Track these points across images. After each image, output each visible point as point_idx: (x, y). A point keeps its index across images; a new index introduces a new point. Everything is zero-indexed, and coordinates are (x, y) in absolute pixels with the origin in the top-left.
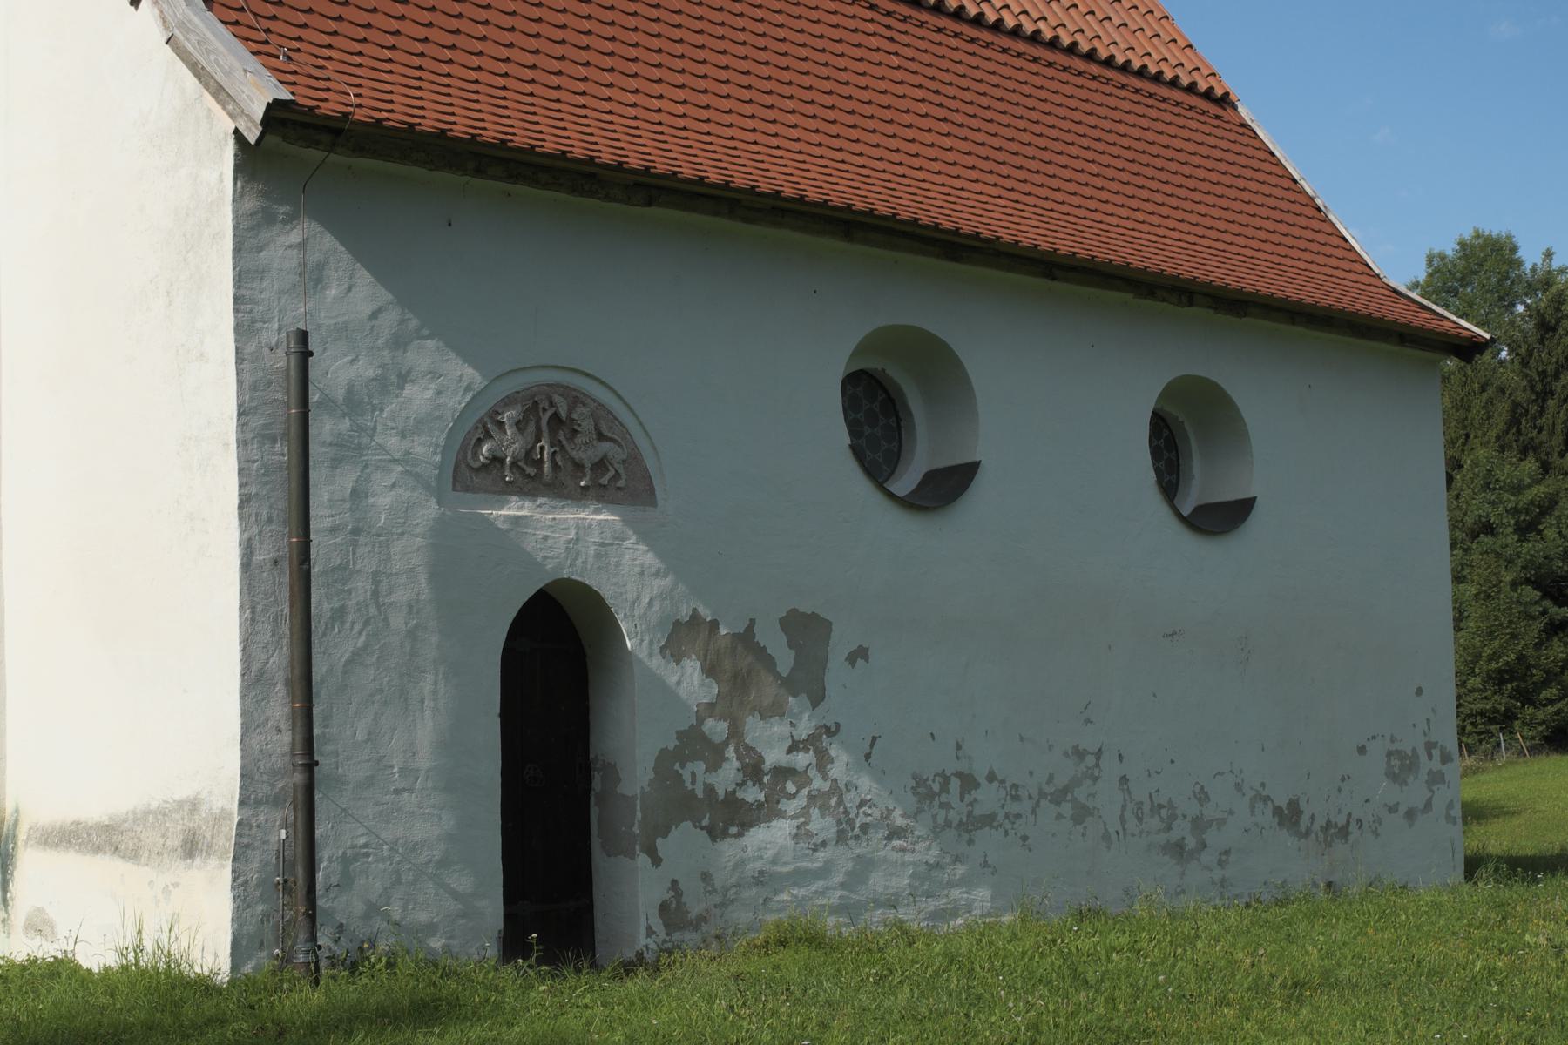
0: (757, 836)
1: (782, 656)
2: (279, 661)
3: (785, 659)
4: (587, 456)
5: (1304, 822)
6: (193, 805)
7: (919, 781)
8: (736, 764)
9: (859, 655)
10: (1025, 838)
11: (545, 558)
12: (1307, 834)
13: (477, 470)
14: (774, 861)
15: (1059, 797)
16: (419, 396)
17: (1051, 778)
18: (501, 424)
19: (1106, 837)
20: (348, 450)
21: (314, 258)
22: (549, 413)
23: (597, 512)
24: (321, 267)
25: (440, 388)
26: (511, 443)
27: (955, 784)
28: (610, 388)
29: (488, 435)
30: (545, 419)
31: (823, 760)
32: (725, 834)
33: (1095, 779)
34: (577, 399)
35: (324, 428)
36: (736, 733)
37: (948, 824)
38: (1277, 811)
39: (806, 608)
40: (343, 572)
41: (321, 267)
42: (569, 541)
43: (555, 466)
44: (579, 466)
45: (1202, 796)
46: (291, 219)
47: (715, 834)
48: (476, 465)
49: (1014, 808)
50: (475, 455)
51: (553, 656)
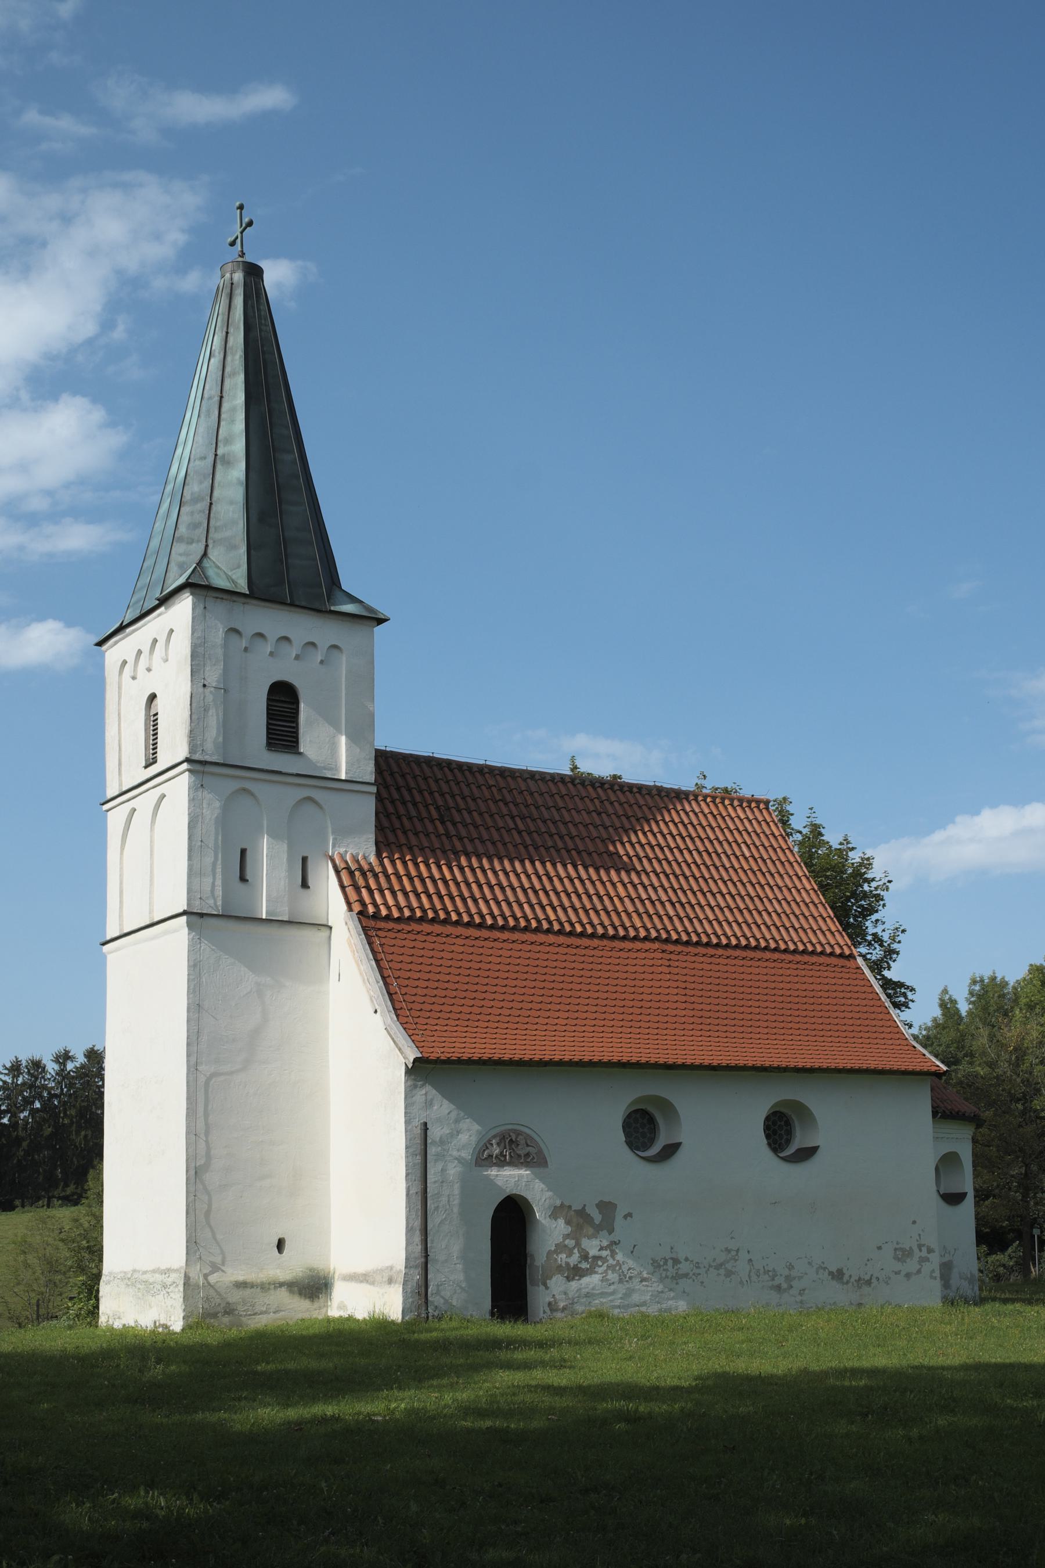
0: (586, 1280)
1: (591, 1218)
2: (418, 1223)
3: (597, 1218)
4: (522, 1152)
5: (846, 1278)
6: (391, 1268)
7: (654, 1261)
8: (578, 1255)
9: (629, 1215)
10: (702, 1283)
12: (848, 1282)
14: (593, 1289)
15: (718, 1267)
16: (464, 1138)
17: (714, 1260)
19: (741, 1282)
20: (440, 1157)
21: (429, 1097)
24: (432, 1100)
25: (468, 1135)
27: (670, 1262)
31: (613, 1254)
32: (573, 1279)
33: (736, 1260)
34: (518, 1133)
35: (432, 1150)
36: (578, 1244)
37: (667, 1277)
38: (831, 1273)
39: (606, 1199)
40: (438, 1195)
41: (432, 1100)
44: (519, 1156)
45: (791, 1267)
46: (422, 1086)
47: (569, 1279)
49: (698, 1271)
51: (511, 1220)
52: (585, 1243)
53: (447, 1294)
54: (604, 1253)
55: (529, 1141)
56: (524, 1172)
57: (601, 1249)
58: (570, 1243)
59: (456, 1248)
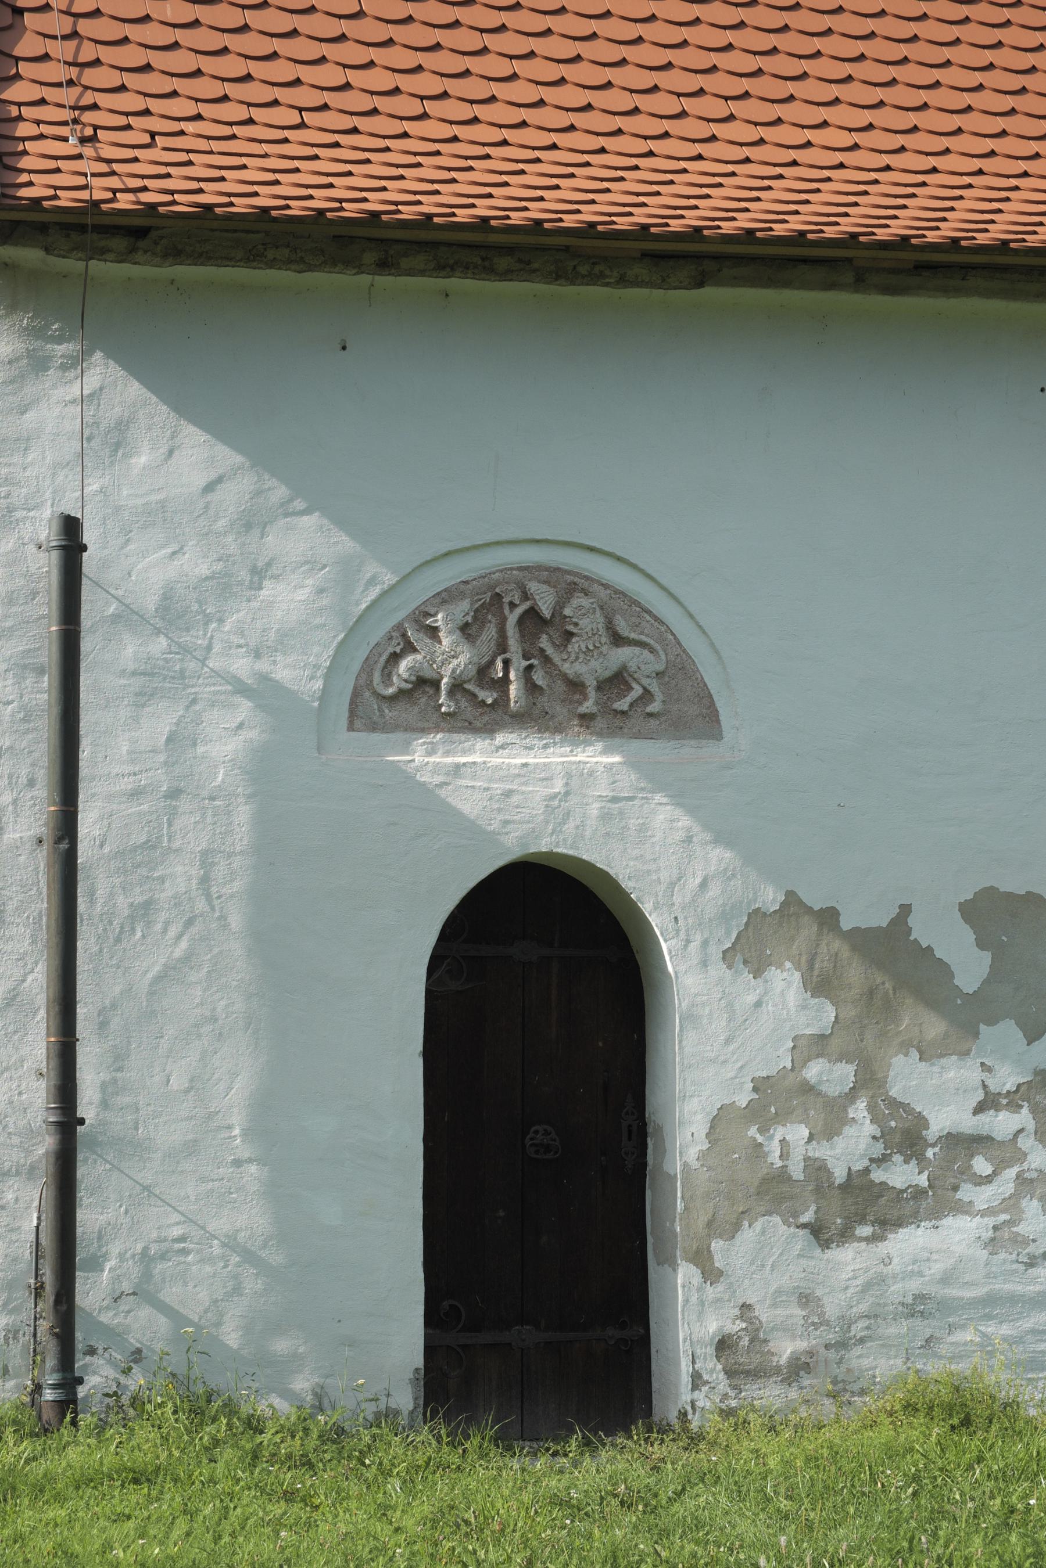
0: (908, 1242)
4: (589, 669)
8: (869, 1129)
11: (506, 823)
13: (393, 699)
14: (946, 1279)
16: (289, 598)
18: (433, 632)
20: (152, 683)
21: (111, 412)
22: (519, 611)
23: (605, 752)
24: (122, 426)
26: (451, 656)
28: (634, 567)
29: (410, 648)
30: (512, 618)
32: (845, 1235)
34: (571, 585)
36: (870, 1080)
39: (1013, 884)
40: (145, 855)
41: (122, 426)
42: (554, 796)
43: (531, 687)
44: (576, 686)
46: (78, 362)
48: (391, 691)
50: (387, 678)
52: (908, 1078)
53: (194, 1289)
54: (1003, 1123)
55: (624, 621)
56: (595, 757)
57: (988, 1103)
58: (832, 1075)
59: (234, 1094)
